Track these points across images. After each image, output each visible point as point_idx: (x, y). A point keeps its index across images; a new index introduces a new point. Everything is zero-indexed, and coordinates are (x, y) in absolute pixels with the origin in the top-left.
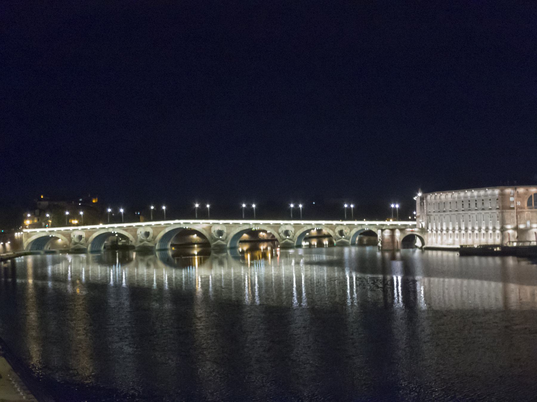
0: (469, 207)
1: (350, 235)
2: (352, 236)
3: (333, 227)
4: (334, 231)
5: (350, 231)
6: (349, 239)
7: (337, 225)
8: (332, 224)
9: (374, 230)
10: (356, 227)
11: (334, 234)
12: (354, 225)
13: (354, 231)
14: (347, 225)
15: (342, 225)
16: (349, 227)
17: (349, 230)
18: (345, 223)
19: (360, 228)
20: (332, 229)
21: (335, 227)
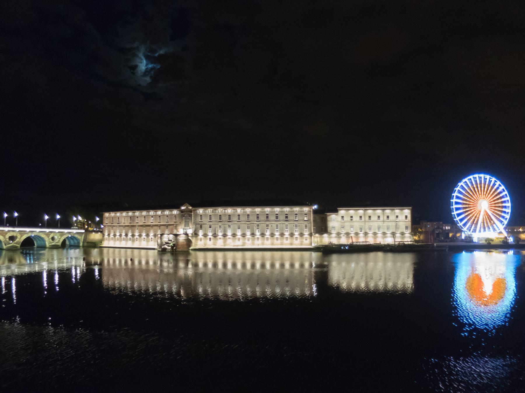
0: (113, 221)
1: (20, 240)
2: (22, 241)
3: (4, 233)
4: (4, 237)
5: (21, 237)
6: (19, 244)
7: (9, 231)
8: (3, 231)
9: (43, 236)
10: (26, 233)
11: (5, 240)
12: (25, 231)
13: (25, 237)
14: (19, 231)
15: (13, 231)
16: (20, 233)
17: (20, 235)
18: (17, 229)
19: (30, 235)
20: (2, 235)
21: (6, 234)
